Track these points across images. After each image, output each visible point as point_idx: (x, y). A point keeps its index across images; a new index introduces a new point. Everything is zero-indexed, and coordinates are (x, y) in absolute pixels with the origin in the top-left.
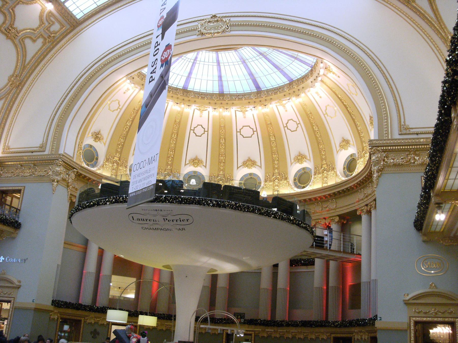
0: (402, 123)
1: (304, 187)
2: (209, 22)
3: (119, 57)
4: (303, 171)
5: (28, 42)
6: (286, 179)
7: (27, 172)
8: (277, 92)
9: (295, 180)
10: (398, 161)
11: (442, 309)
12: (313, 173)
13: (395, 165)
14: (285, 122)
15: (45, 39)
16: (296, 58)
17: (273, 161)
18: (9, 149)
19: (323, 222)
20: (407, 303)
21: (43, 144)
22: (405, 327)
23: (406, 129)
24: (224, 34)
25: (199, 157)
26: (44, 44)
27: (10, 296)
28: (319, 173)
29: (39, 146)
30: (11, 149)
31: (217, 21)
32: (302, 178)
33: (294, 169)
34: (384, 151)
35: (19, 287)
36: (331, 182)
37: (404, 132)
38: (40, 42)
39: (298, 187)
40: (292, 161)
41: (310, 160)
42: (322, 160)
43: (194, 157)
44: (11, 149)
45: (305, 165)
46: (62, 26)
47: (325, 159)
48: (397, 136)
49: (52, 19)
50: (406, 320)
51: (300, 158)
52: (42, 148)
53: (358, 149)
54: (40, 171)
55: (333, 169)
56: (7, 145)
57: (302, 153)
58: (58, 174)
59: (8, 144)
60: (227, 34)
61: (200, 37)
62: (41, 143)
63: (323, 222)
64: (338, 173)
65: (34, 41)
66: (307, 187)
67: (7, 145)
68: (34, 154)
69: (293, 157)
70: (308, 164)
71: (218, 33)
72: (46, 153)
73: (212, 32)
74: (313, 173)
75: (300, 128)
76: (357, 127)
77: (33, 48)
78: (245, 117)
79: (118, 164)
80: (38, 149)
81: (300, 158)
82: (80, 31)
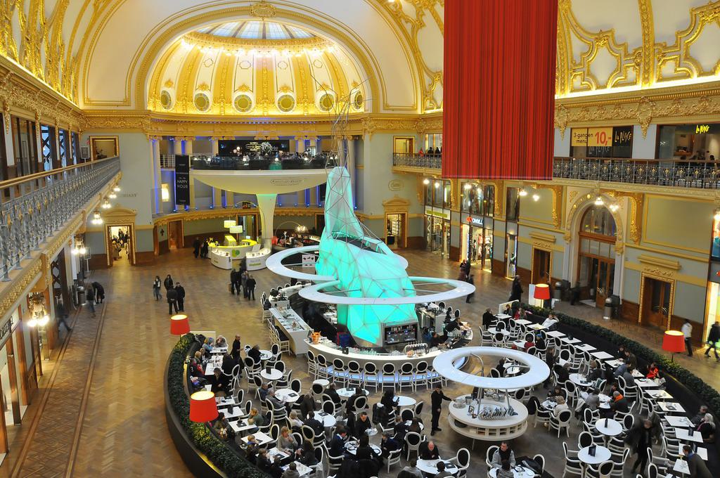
1: (287, 111)
7: (118, 124)
8: (279, 42)
11: (401, 207)
12: (296, 101)
19: (305, 138)
22: (383, 217)
25: (206, 83)
32: (286, 103)
35: (135, 215)
37: (386, 108)
39: (282, 110)
48: (382, 111)
51: (285, 88)
52: (126, 102)
54: (129, 123)
55: (313, 102)
63: (305, 138)
70: (293, 95)
72: (132, 107)
74: (296, 101)
78: (246, 55)
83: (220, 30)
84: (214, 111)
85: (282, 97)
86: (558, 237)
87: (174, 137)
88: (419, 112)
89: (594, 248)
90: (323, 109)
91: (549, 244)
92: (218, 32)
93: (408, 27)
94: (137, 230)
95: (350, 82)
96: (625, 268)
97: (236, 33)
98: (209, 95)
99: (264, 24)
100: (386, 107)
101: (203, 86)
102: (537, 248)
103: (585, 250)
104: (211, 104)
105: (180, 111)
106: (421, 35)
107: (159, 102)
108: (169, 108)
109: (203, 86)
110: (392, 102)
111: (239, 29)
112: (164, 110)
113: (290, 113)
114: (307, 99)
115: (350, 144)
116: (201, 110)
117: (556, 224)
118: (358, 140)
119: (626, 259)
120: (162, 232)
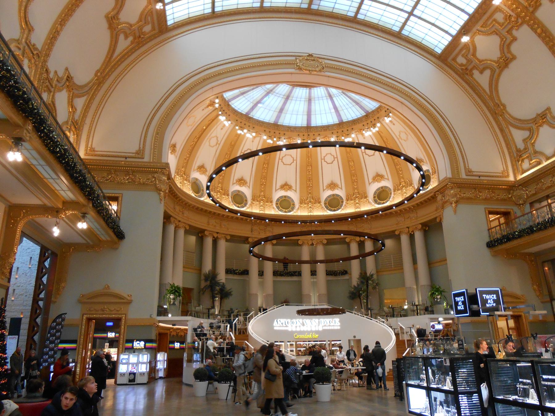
0: (467, 167)
2: (307, 59)
3: (219, 74)
4: (332, 197)
5: (122, 37)
7: (124, 179)
9: (325, 204)
13: (469, 199)
15: (135, 39)
16: (357, 103)
18: (94, 151)
21: (139, 150)
23: (470, 172)
24: (319, 73)
25: (245, 178)
26: (132, 43)
27: (119, 313)
29: (134, 152)
30: (97, 151)
31: (314, 60)
32: (334, 202)
33: (326, 194)
35: (129, 302)
37: (469, 174)
38: (131, 38)
40: (325, 188)
41: (341, 189)
42: (354, 189)
43: (240, 177)
44: (97, 151)
45: (337, 192)
46: (153, 28)
47: (357, 189)
49: (149, 18)
51: (333, 185)
52: (140, 153)
53: (394, 183)
55: (366, 197)
56: (89, 146)
57: (334, 182)
59: (92, 145)
60: (322, 73)
61: (298, 71)
62: (137, 149)
64: (370, 200)
65: (126, 37)
66: (340, 210)
67: (89, 146)
69: (325, 184)
70: (341, 192)
71: (315, 71)
72: (146, 159)
73: (311, 69)
75: (336, 162)
76: (395, 166)
77: (123, 44)
80: (134, 155)
82: (169, 39)
85: (329, 197)
88: (511, 178)
94: (128, 326)
97: (278, 117)
98: (247, 191)
100: (469, 172)
111: (281, 110)
114: (358, 194)
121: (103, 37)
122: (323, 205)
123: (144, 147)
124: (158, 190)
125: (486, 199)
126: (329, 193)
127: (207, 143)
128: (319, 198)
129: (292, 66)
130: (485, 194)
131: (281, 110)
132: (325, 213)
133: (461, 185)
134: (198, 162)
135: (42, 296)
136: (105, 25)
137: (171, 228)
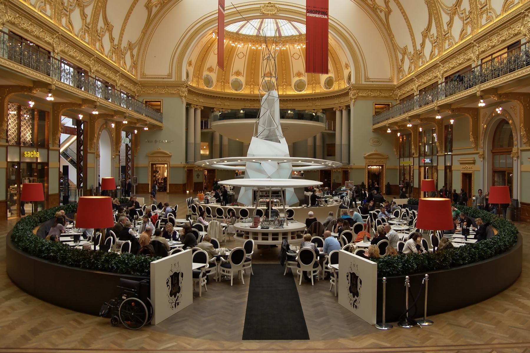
1: (301, 91)
6: (291, 85)
9: (295, 86)
10: (364, 95)
13: (362, 96)
14: (292, 54)
17: (283, 74)
20: (365, 158)
23: (368, 79)
28: (311, 85)
32: (300, 86)
33: (295, 80)
34: (358, 89)
35: (170, 156)
36: (318, 91)
48: (364, 83)
50: (364, 165)
52: (170, 75)
55: (319, 83)
58: (183, 92)
68: (165, 80)
72: (173, 79)
79: (198, 78)
81: (299, 74)
83: (246, 29)
84: (245, 91)
86: (476, 157)
87: (213, 108)
88: (395, 83)
89: (502, 162)
90: (327, 88)
91: (471, 166)
92: (244, 31)
93: (382, 15)
94: (171, 167)
95: (343, 64)
96: (521, 172)
98: (242, 79)
99: (277, 23)
100: (367, 79)
101: (238, 73)
102: (466, 172)
103: (497, 166)
104: (244, 87)
105: (219, 90)
106: (391, 18)
107: (202, 82)
108: (211, 87)
109: (238, 73)
110: (371, 75)
112: (206, 88)
113: (303, 92)
115: (344, 112)
116: (236, 90)
117: (473, 146)
118: (348, 108)
119: (522, 163)
120: (198, 176)
121: (145, 13)
122: (293, 87)
123: (172, 73)
124: (181, 97)
125: (374, 97)
126: (297, 79)
127: (213, 53)
128: (291, 82)
129: (258, 11)
130: (373, 94)
131: (260, 28)
132: (294, 93)
133: (359, 88)
134: (207, 65)
135: (129, 153)
136: (145, 8)
137: (192, 111)
